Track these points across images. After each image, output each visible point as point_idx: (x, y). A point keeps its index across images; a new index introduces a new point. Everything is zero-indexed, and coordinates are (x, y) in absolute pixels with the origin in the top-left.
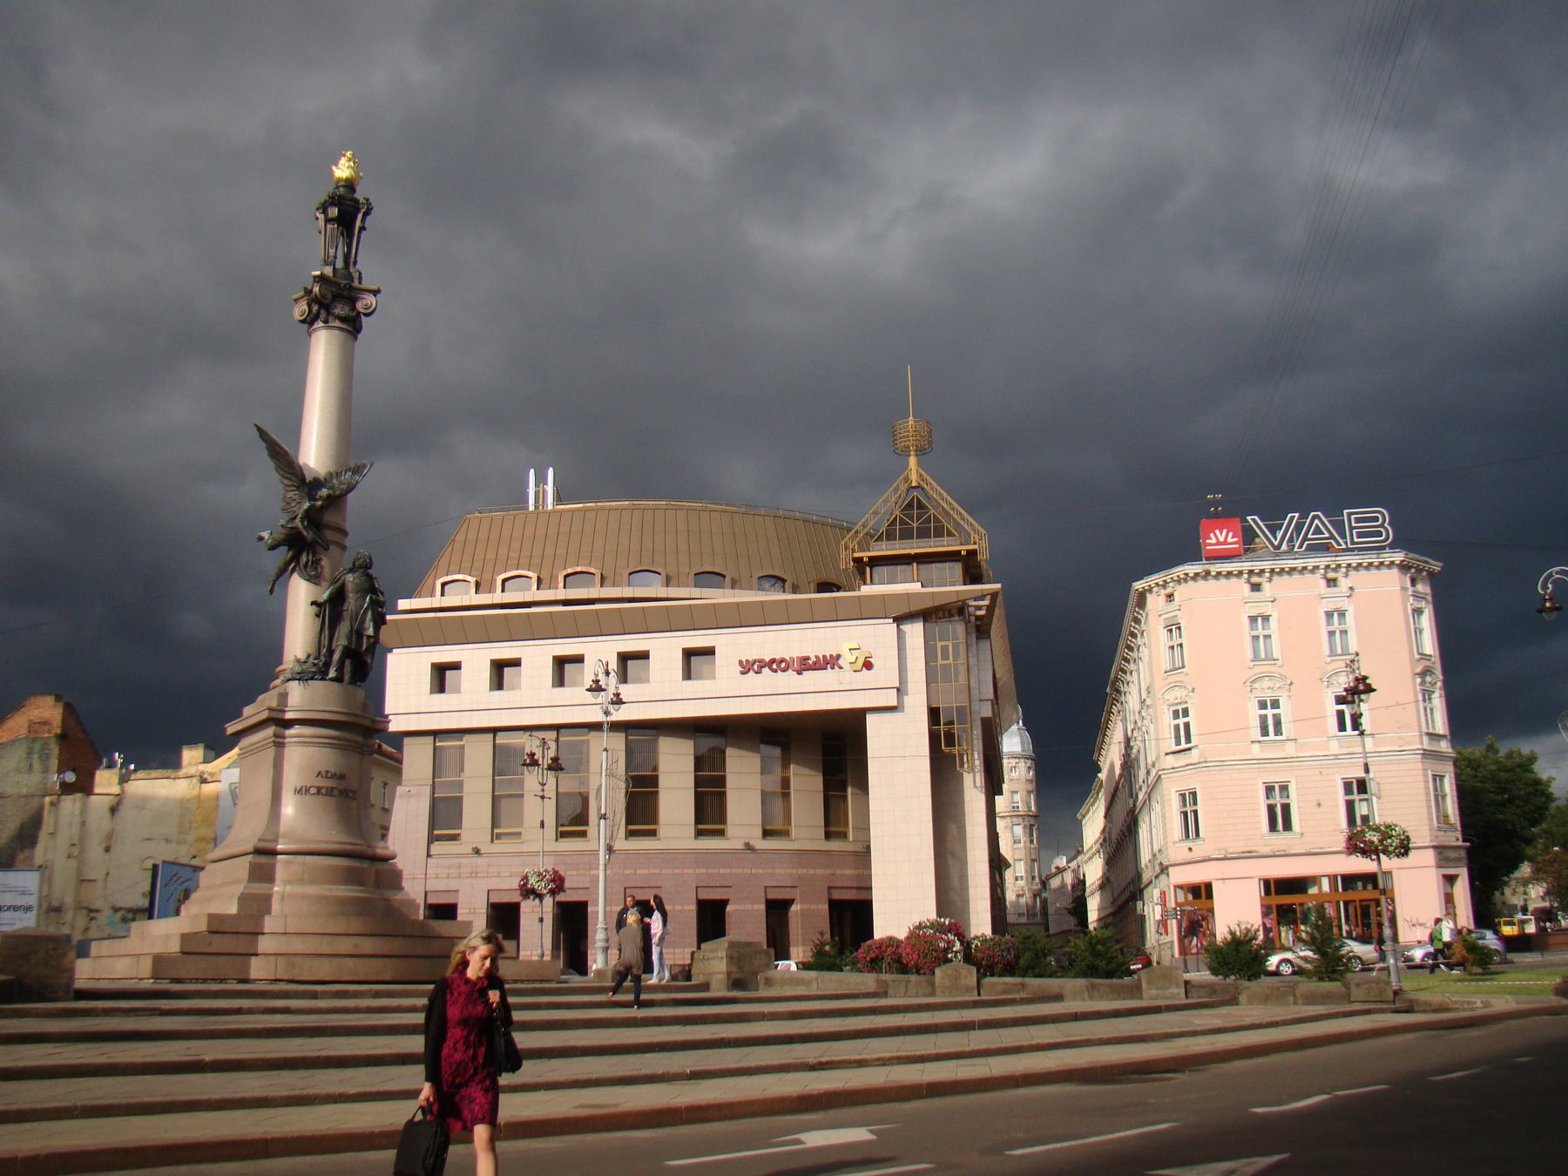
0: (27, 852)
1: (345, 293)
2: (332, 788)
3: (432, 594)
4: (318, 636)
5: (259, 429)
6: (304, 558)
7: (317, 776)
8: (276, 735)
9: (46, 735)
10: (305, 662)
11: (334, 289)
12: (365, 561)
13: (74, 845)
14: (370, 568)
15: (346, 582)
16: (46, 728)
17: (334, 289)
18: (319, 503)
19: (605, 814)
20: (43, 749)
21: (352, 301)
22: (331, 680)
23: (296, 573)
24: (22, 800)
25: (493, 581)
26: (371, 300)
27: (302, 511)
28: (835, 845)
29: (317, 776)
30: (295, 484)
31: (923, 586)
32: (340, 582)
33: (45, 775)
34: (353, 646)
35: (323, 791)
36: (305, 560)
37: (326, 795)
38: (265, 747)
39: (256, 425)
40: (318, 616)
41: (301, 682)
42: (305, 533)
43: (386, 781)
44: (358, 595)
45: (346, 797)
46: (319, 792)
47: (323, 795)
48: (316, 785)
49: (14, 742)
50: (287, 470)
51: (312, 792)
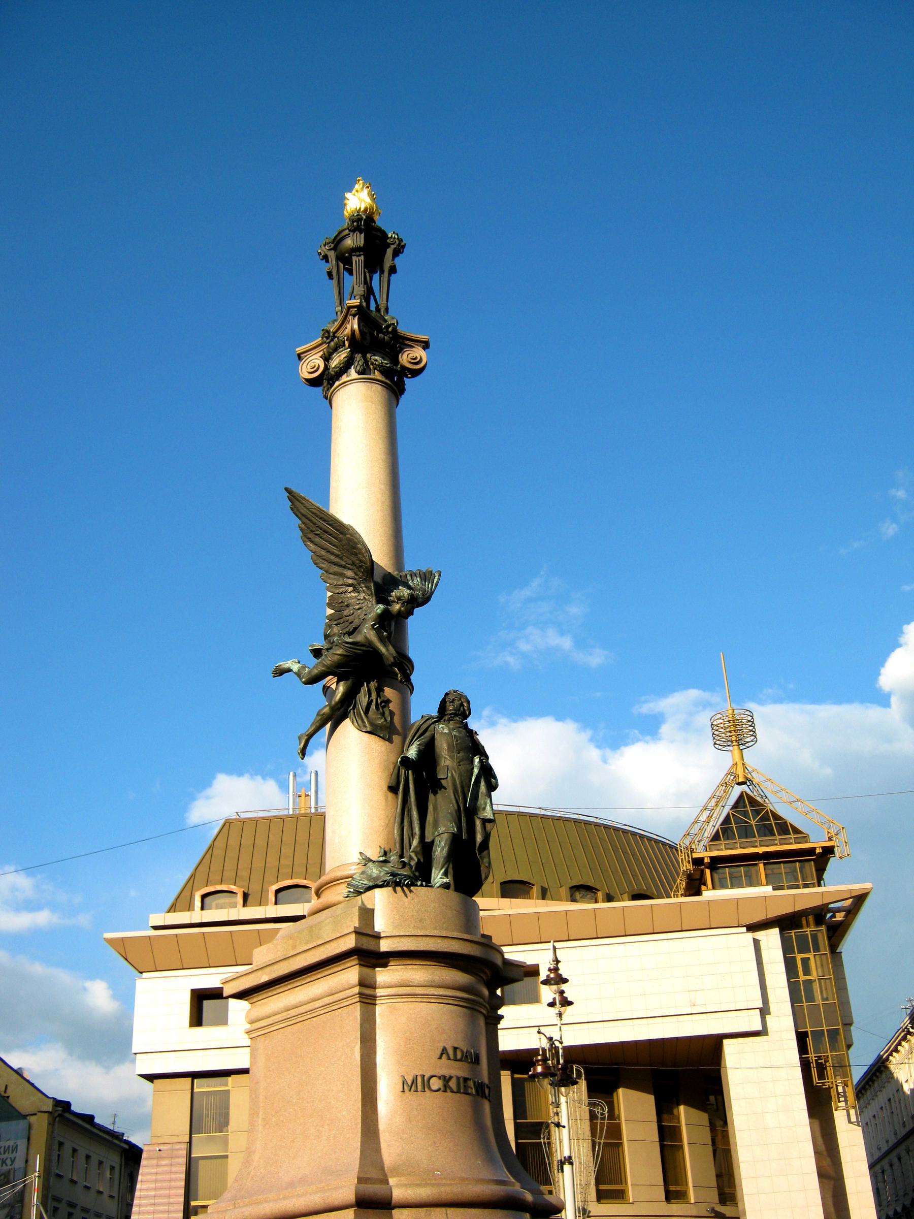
3: (190, 907)
4: (398, 819)
6: (363, 698)
7: (440, 1058)
8: (362, 984)
10: (385, 862)
12: (462, 705)
15: (437, 737)
18: (397, 607)
19: (570, 1157)
22: (446, 886)
23: (347, 722)
25: (263, 892)
26: (419, 352)
27: (372, 615)
28: (676, 1208)
29: (440, 1058)
30: (350, 581)
31: (774, 889)
32: (428, 734)
35: (453, 1084)
36: (365, 701)
37: (458, 1092)
38: (333, 1005)
39: (287, 489)
40: (393, 789)
41: (398, 889)
42: (383, 649)
43: (77, 1147)
44: (461, 754)
46: (446, 1088)
47: (452, 1092)
50: (337, 560)
51: (435, 1087)
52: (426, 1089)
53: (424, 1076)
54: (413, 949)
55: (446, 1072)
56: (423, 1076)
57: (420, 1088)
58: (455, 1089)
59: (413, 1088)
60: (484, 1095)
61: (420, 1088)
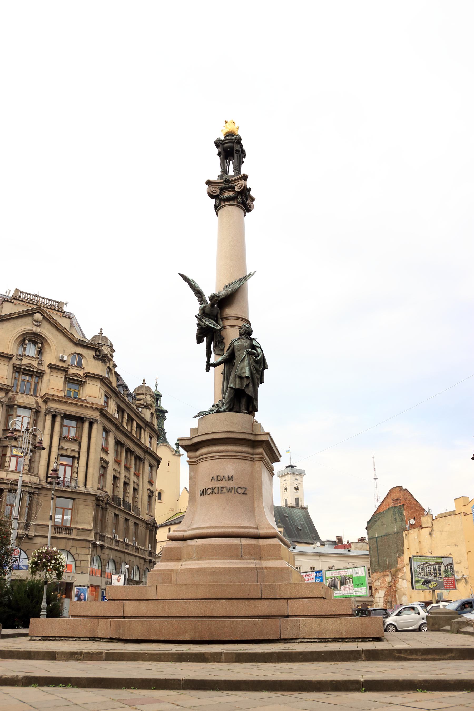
0: (401, 557)
1: (227, 186)
2: (223, 487)
5: (182, 275)
9: (399, 504)
11: (220, 186)
13: (418, 552)
14: (251, 335)
16: (398, 501)
17: (220, 186)
20: (399, 511)
21: (233, 188)
24: (396, 535)
29: (211, 481)
33: (402, 522)
34: (237, 387)
35: (216, 491)
37: (218, 493)
39: (179, 274)
45: (235, 493)
47: (216, 494)
48: (211, 487)
49: (387, 510)
51: (209, 493)
52: (206, 494)
53: (205, 489)
54: (200, 440)
55: (214, 486)
56: (205, 489)
57: (204, 494)
58: (217, 492)
59: (203, 494)
60: (236, 493)
61: (204, 494)
